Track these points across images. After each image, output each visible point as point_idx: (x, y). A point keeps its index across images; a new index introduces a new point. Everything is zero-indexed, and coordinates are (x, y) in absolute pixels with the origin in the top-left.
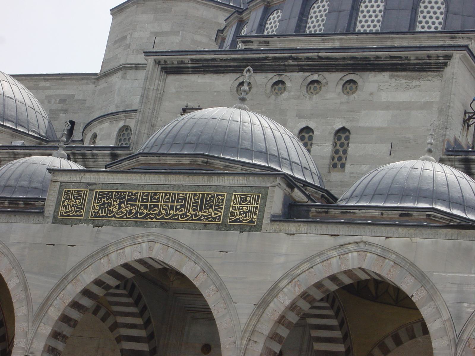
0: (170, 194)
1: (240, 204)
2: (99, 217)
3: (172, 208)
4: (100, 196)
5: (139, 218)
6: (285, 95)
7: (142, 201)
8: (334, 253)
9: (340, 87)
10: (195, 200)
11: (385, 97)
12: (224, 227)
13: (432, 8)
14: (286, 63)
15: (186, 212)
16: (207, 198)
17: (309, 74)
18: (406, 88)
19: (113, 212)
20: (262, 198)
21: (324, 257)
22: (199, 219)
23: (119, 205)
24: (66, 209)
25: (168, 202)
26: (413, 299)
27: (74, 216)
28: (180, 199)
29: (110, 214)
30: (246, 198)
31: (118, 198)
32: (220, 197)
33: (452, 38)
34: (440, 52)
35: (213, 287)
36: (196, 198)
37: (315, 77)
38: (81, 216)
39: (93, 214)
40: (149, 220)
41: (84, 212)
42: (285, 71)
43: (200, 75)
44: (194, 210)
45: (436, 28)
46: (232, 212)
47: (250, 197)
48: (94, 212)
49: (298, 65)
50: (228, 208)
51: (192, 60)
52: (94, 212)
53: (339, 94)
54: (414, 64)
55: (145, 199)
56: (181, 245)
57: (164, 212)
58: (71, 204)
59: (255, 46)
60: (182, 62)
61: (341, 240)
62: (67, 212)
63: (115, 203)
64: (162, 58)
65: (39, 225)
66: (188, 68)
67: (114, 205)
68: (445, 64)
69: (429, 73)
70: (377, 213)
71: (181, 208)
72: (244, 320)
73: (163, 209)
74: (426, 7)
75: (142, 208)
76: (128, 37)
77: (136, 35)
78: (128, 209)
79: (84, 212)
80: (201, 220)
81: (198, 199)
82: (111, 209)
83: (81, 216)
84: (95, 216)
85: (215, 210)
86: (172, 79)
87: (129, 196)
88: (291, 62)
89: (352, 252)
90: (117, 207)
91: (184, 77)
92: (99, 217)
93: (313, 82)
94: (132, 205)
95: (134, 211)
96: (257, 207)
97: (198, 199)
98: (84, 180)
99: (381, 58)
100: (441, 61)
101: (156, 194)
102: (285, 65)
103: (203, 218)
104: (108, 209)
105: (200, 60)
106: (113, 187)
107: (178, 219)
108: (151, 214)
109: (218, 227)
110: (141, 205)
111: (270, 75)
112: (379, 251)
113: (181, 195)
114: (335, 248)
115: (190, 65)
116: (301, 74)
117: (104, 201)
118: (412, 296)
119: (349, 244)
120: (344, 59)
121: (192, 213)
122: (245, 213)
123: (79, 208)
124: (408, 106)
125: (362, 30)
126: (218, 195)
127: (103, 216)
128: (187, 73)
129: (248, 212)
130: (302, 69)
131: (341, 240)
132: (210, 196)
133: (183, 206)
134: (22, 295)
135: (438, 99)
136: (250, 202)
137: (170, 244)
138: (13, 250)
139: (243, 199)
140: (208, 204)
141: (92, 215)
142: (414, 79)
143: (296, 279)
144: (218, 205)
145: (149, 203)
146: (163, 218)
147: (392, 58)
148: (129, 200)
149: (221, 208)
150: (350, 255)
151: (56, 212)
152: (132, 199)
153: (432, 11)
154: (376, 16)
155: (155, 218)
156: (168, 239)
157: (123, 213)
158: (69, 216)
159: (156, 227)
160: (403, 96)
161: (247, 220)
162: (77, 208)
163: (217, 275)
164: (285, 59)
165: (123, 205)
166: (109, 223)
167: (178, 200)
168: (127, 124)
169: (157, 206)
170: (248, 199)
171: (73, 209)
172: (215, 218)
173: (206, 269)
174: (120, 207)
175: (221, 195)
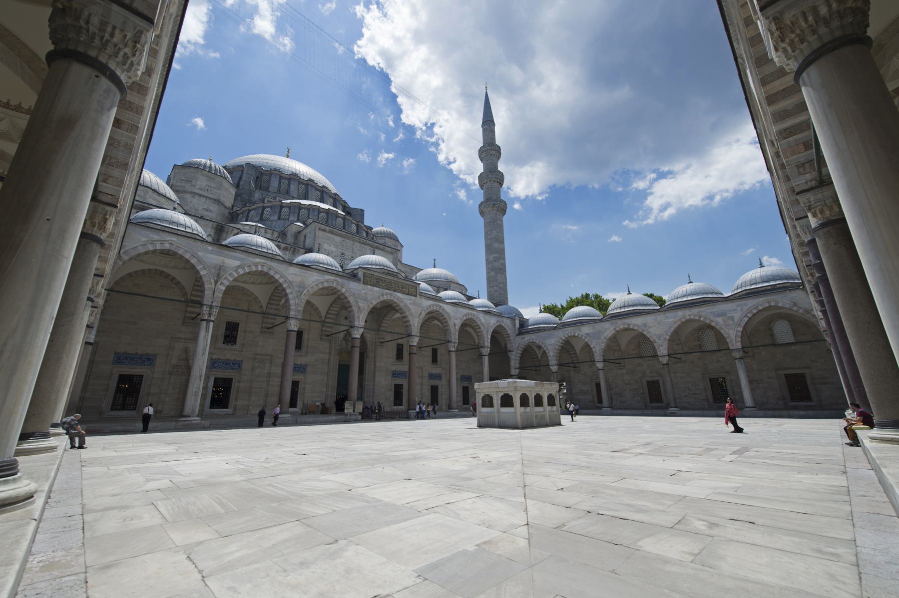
4: (376, 279)
51: (329, 229)
76: (194, 181)
77: (198, 183)
109: (407, 294)
123: (370, 281)
151: (363, 281)
152: (385, 282)
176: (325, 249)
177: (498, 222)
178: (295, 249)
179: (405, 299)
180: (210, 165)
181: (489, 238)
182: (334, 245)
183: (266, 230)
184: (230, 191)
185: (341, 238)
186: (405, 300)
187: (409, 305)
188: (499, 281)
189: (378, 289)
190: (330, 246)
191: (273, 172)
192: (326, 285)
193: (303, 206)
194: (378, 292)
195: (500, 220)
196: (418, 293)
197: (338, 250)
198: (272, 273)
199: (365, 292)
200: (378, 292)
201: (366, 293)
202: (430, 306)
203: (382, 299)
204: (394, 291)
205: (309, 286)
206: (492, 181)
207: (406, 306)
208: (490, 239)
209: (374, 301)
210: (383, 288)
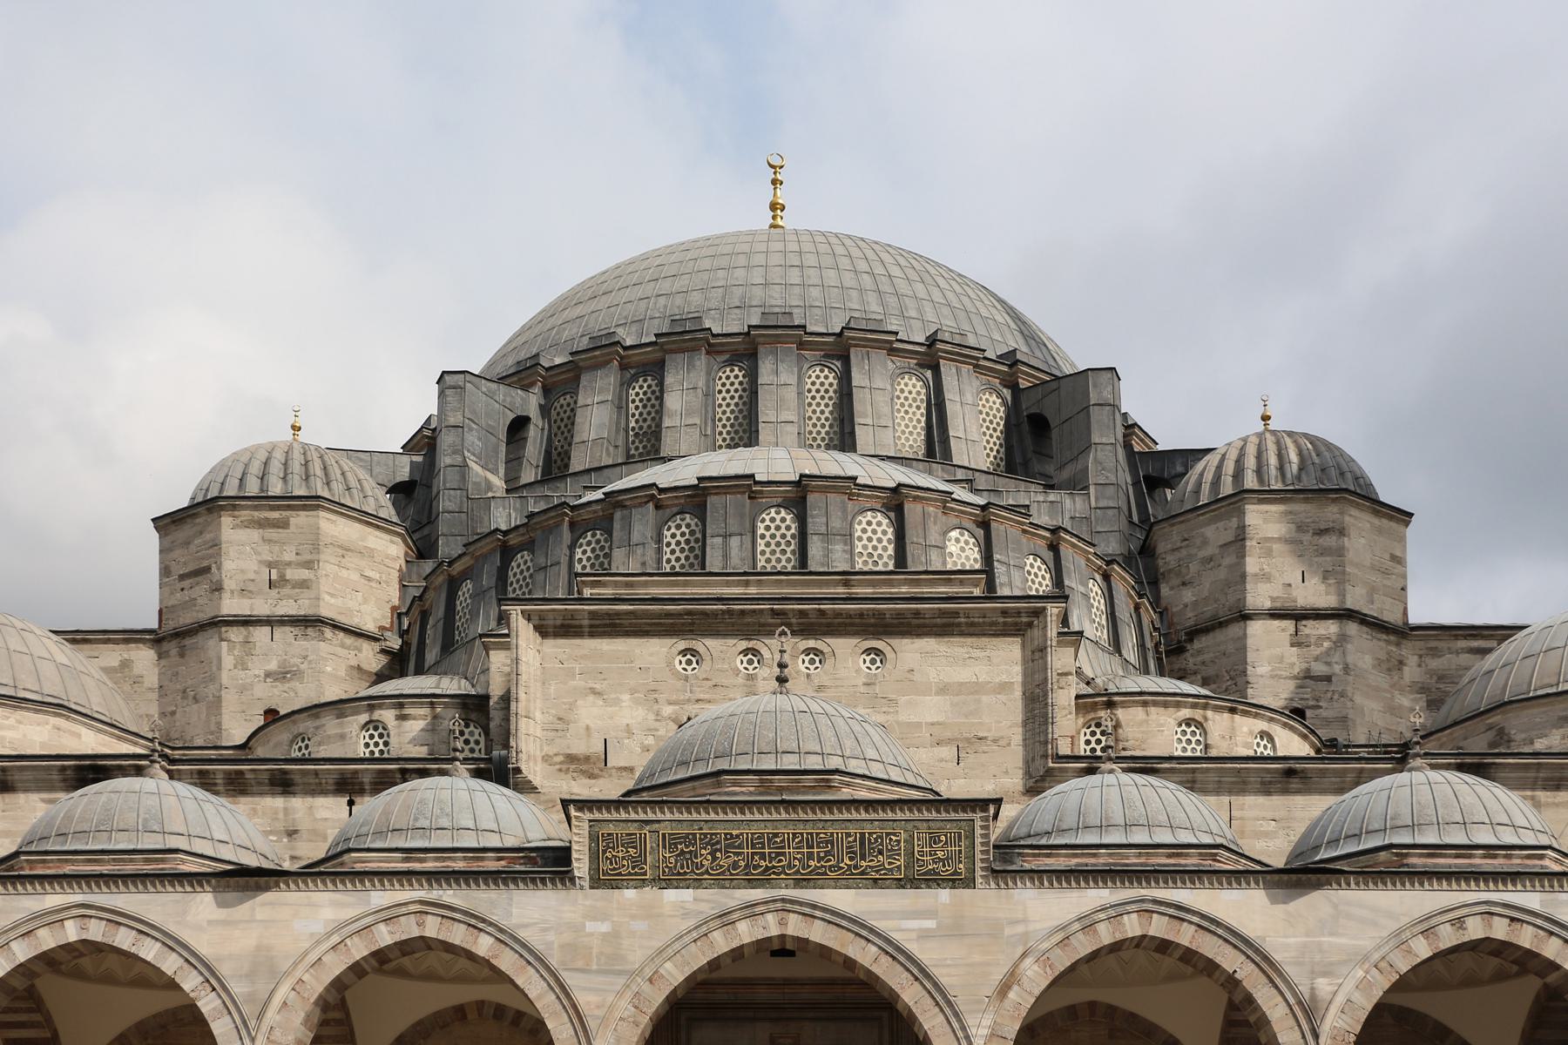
0: (802, 834)
1: (931, 846)
2: (679, 874)
4: (671, 842)
5: (753, 874)
8: (1102, 916)
10: (849, 842)
16: (869, 840)
19: (702, 866)
20: (966, 837)
23: (713, 854)
24: (611, 863)
25: (802, 847)
26: (1236, 975)
27: (630, 874)
28: (822, 842)
29: (697, 869)
30: (939, 837)
31: (707, 844)
32: (894, 838)
36: (850, 839)
37: (811, 643)
39: (667, 870)
40: (773, 876)
41: (647, 868)
44: (851, 859)
45: (886, 564)
46: (918, 859)
47: (946, 836)
48: (667, 866)
52: (667, 866)
55: (758, 843)
58: (620, 854)
62: (614, 869)
63: (703, 852)
66: (581, 626)
67: (701, 855)
68: (1030, 625)
71: (826, 856)
73: (795, 858)
74: (864, 531)
75: (756, 858)
78: (730, 861)
80: (867, 874)
81: (855, 840)
82: (699, 860)
83: (645, 874)
87: (726, 839)
90: (709, 857)
92: (679, 874)
95: (742, 864)
96: (960, 851)
97: (855, 840)
99: (841, 614)
100: (1025, 620)
101: (776, 835)
103: (869, 870)
104: (692, 861)
106: (692, 825)
108: (774, 867)
109: (900, 884)
111: (731, 642)
112: (1171, 911)
113: (822, 835)
117: (682, 850)
118: (1235, 971)
120: (861, 614)
121: (849, 863)
122: (943, 860)
123: (639, 861)
124: (976, 689)
125: (866, 569)
126: (888, 834)
127: (685, 873)
129: (947, 859)
132: (875, 836)
136: (946, 843)
139: (934, 840)
140: (873, 849)
141: (664, 872)
143: (1045, 957)
144: (892, 850)
145: (767, 851)
146: (798, 872)
148: (727, 846)
149: (899, 855)
157: (721, 867)
158: (620, 874)
159: (787, 887)
161: (947, 870)
162: (632, 862)
165: (718, 855)
167: (818, 843)
169: (784, 854)
170: (943, 838)
171: (625, 863)
172: (891, 870)
174: (714, 858)
175: (894, 834)
176: (588, 728)
179: (886, 915)
182: (633, 692)
185: (668, 641)
186: (880, 925)
187: (913, 947)
189: (686, 895)
190: (617, 702)
192: (385, 936)
194: (686, 915)
197: (658, 717)
198: (124, 939)
199: (604, 927)
200: (686, 915)
201: (614, 936)
202: (1088, 923)
203: (721, 943)
204: (799, 883)
205: (295, 964)
207: (895, 951)
209: (668, 965)
210: (720, 883)
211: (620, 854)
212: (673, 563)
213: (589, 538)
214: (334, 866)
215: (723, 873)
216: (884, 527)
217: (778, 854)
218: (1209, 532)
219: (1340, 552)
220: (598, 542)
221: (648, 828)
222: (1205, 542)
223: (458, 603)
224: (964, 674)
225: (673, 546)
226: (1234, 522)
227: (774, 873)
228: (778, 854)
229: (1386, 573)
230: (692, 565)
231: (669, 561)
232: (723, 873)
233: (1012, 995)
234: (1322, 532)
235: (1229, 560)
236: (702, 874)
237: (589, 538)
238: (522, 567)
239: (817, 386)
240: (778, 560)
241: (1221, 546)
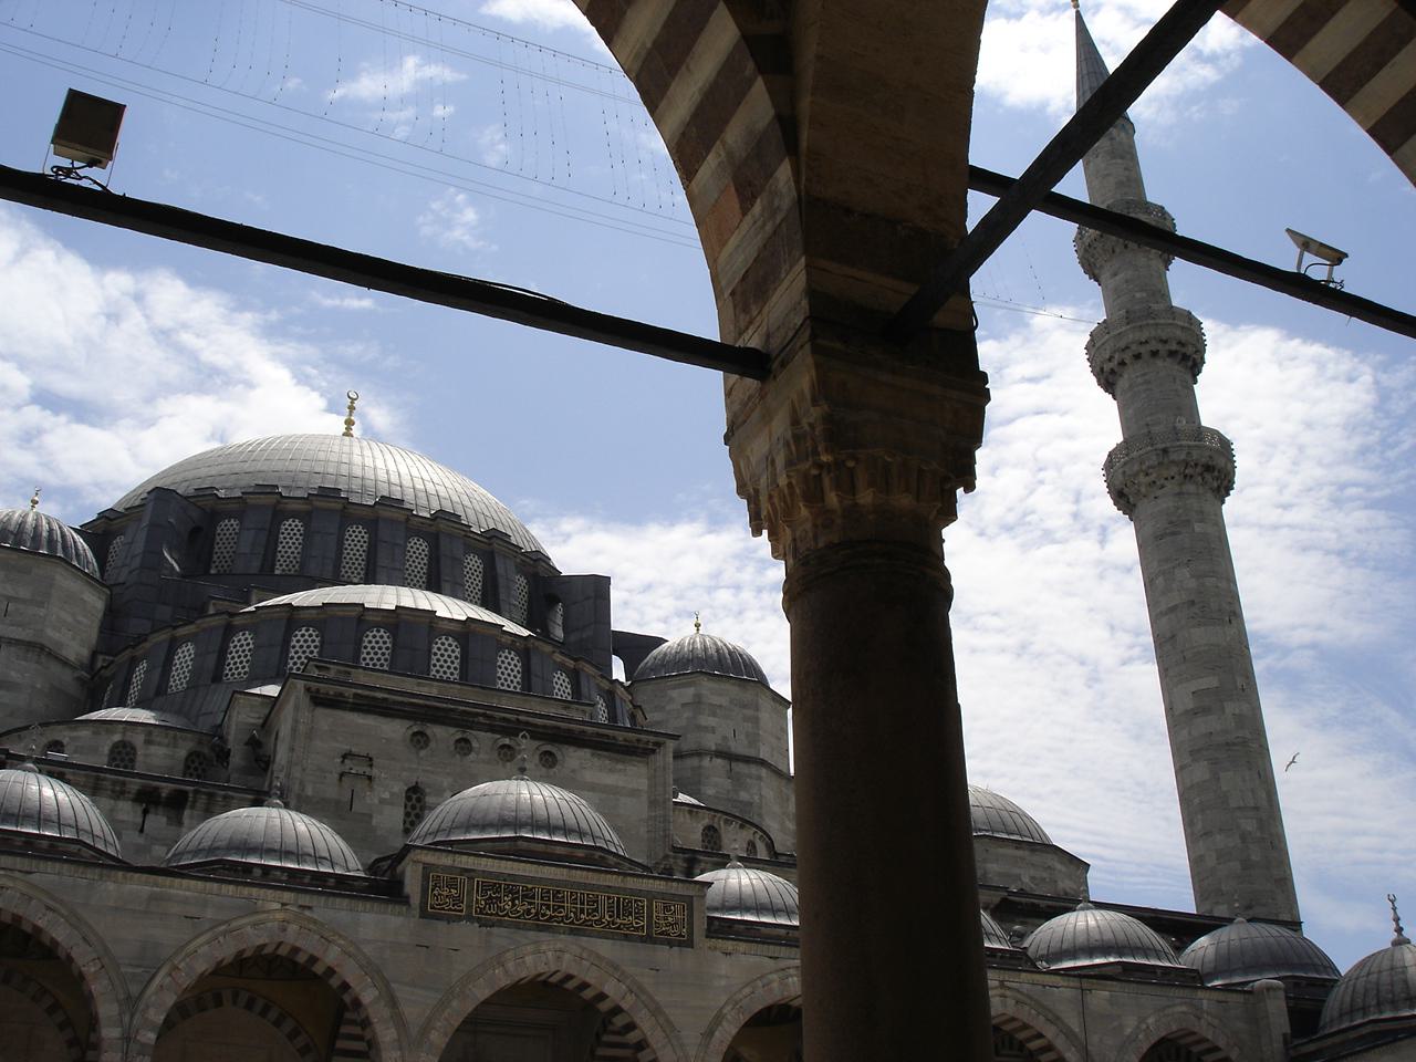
2: (487, 914)
3: (582, 911)
4: (485, 887)
6: (472, 756)
7: (542, 899)
9: (537, 757)
11: (589, 776)
12: (649, 939)
13: (446, 650)
14: (476, 720)
15: (601, 918)
17: (499, 736)
18: (611, 771)
21: (765, 981)
22: (618, 928)
23: (513, 900)
27: (450, 910)
33: (565, 708)
34: (652, 739)
35: (644, 1011)
36: (611, 901)
38: (461, 911)
42: (471, 728)
43: (361, 714)
44: (610, 917)
45: (515, 687)
49: (489, 725)
50: (650, 917)
51: (356, 695)
53: (536, 765)
54: (621, 746)
56: (598, 956)
57: (572, 915)
59: (327, 675)
60: (341, 695)
61: (783, 964)
64: (313, 685)
65: (401, 919)
68: (653, 751)
69: (634, 758)
70: (783, 932)
72: (692, 1052)
79: (464, 906)
83: (461, 911)
84: (481, 913)
85: (636, 918)
86: (320, 711)
88: (481, 719)
89: (792, 976)
91: (339, 713)
93: (503, 746)
94: (530, 904)
98: (456, 864)
101: (558, 892)
102: (473, 722)
105: (367, 697)
107: (591, 926)
109: (642, 940)
110: (542, 904)
111: (452, 730)
114: (777, 971)
115: (351, 700)
116: (489, 734)
119: (789, 968)
120: (544, 727)
122: (671, 925)
123: (458, 900)
126: (636, 901)
127: (492, 914)
128: (344, 709)
130: (492, 729)
131: (783, 964)
133: (596, 910)
134: (386, 1013)
135: (646, 788)
137: (585, 955)
138: (367, 949)
139: (667, 908)
142: (618, 761)
146: (572, 923)
147: (598, 734)
150: (790, 979)
153: (373, 644)
154: (452, 662)
155: (562, 921)
156: (584, 949)
158: (443, 909)
159: (564, 933)
160: (610, 779)
163: (651, 998)
164: (477, 714)
166: (500, 924)
168: (127, 738)
169: (563, 907)
172: (637, 929)
173: (635, 989)
174: (514, 905)
177: (1198, 527)
178: (211, 796)
180: (36, 528)
181: (1163, 607)
183: (150, 733)
184: (82, 599)
185: (407, 723)
188: (1233, 804)
191: (252, 500)
193: (303, 615)
195: (1201, 521)
196: (700, 926)
206: (1146, 356)
208: (1173, 609)
210: (517, 926)
211: (445, 893)
212: (368, 661)
213: (303, 632)
214: (198, 871)
215: (518, 917)
216: (516, 661)
217: (560, 907)
218: (674, 694)
219: (756, 721)
220: (310, 636)
221: (467, 874)
222: (671, 700)
223: (176, 657)
224: (610, 779)
225: (369, 649)
226: (691, 691)
227: (555, 921)
228: (560, 907)
229: (779, 739)
230: (382, 665)
231: (365, 659)
232: (518, 917)
233: (717, 1033)
234: (745, 706)
235: (687, 714)
236: (503, 916)
237: (303, 632)
238: (243, 642)
239: (294, 540)
240: (445, 673)
241: (684, 705)
